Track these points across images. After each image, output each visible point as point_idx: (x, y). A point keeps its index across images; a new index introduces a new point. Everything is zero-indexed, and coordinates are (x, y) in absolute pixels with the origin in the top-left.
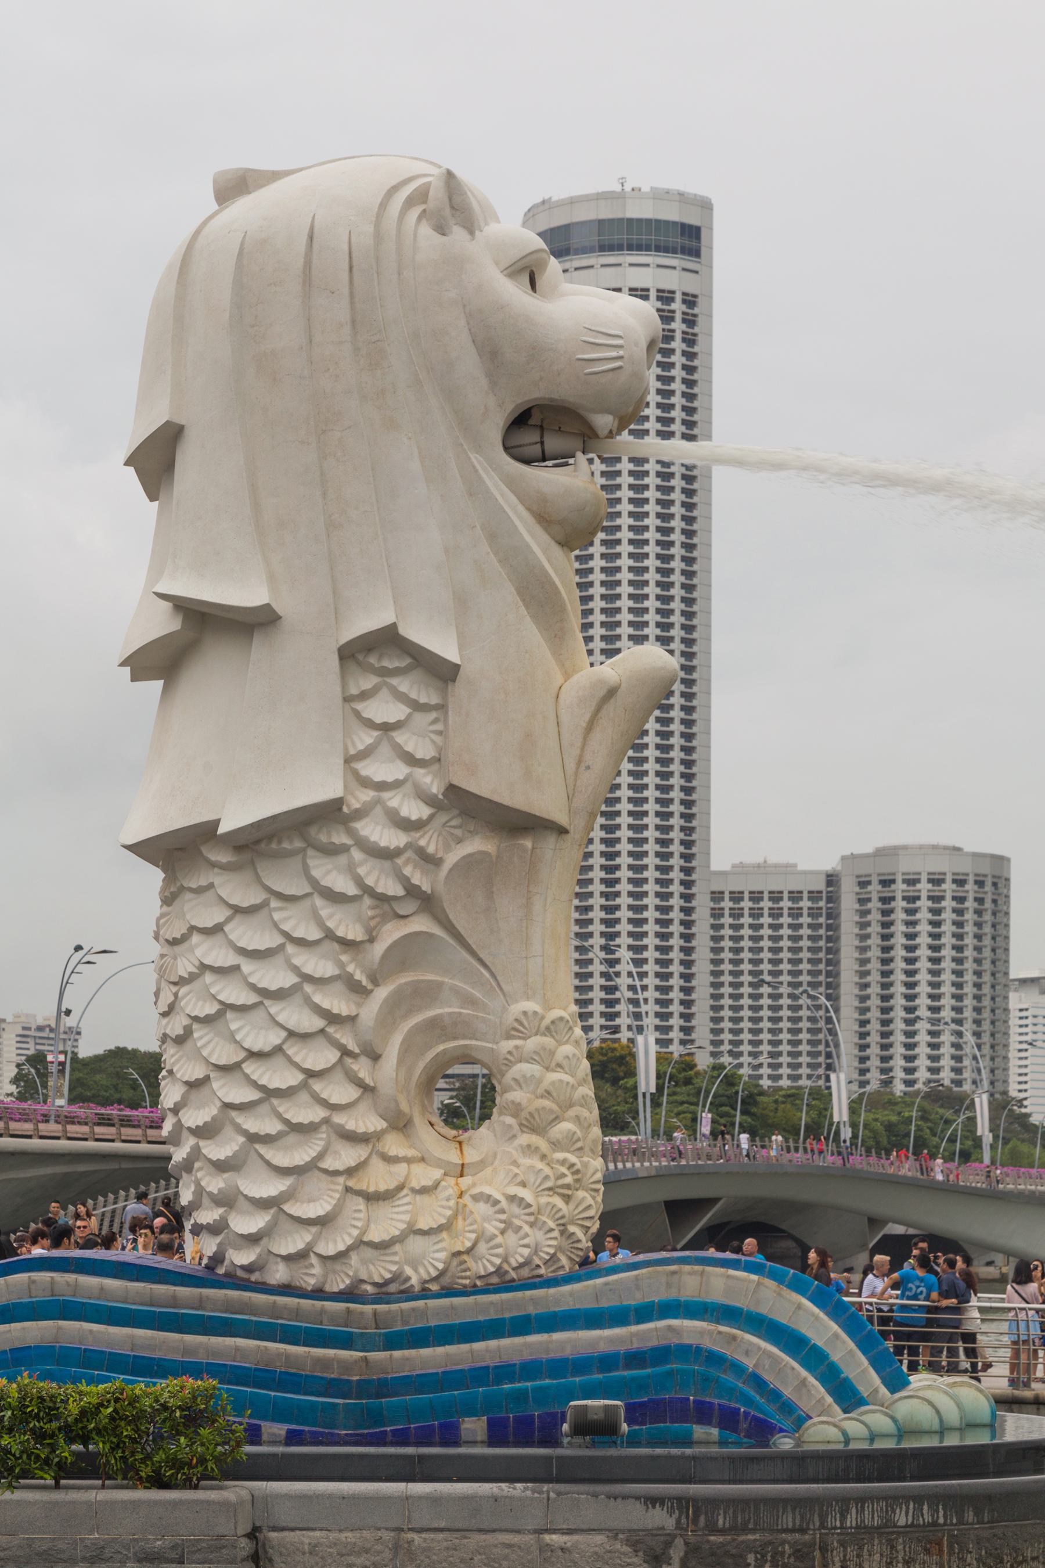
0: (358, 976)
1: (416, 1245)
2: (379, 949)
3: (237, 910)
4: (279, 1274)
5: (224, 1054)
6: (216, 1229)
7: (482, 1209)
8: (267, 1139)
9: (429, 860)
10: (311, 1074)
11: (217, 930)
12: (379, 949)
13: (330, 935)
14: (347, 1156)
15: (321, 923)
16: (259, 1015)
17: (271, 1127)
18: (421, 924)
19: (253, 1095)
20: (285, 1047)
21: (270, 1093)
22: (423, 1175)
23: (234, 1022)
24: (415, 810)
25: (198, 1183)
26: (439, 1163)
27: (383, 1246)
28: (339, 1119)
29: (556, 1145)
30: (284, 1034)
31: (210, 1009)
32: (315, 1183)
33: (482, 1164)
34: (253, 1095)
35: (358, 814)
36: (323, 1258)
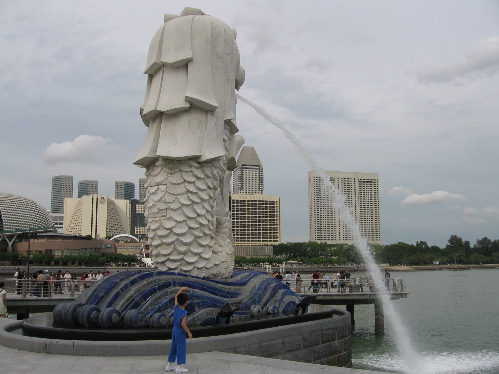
1: (222, 265)
5: (193, 215)
11: (193, 183)
16: (200, 206)
19: (197, 226)
31: (190, 203)
34: (197, 226)
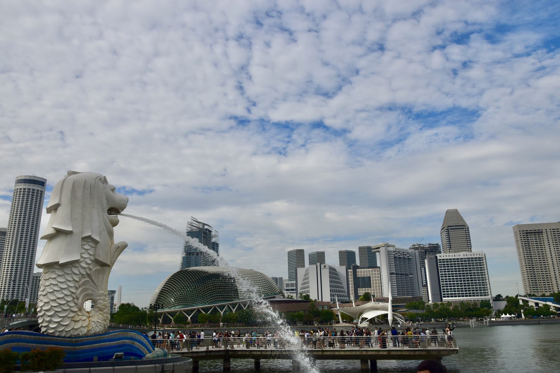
1: (82, 329)
2: (81, 282)
3: (59, 275)
4: (57, 334)
5: (53, 298)
6: (45, 327)
7: (93, 323)
8: (58, 312)
9: (90, 269)
10: (68, 301)
11: (55, 278)
12: (81, 282)
13: (74, 280)
14: (72, 315)
15: (73, 278)
17: (59, 310)
18: (87, 279)
21: (60, 304)
22: (85, 318)
24: (89, 262)
25: (44, 319)
26: (86, 316)
27: (77, 329)
28: (71, 309)
29: (104, 313)
31: (52, 290)
32: (66, 319)
33: (92, 317)
35: (81, 262)
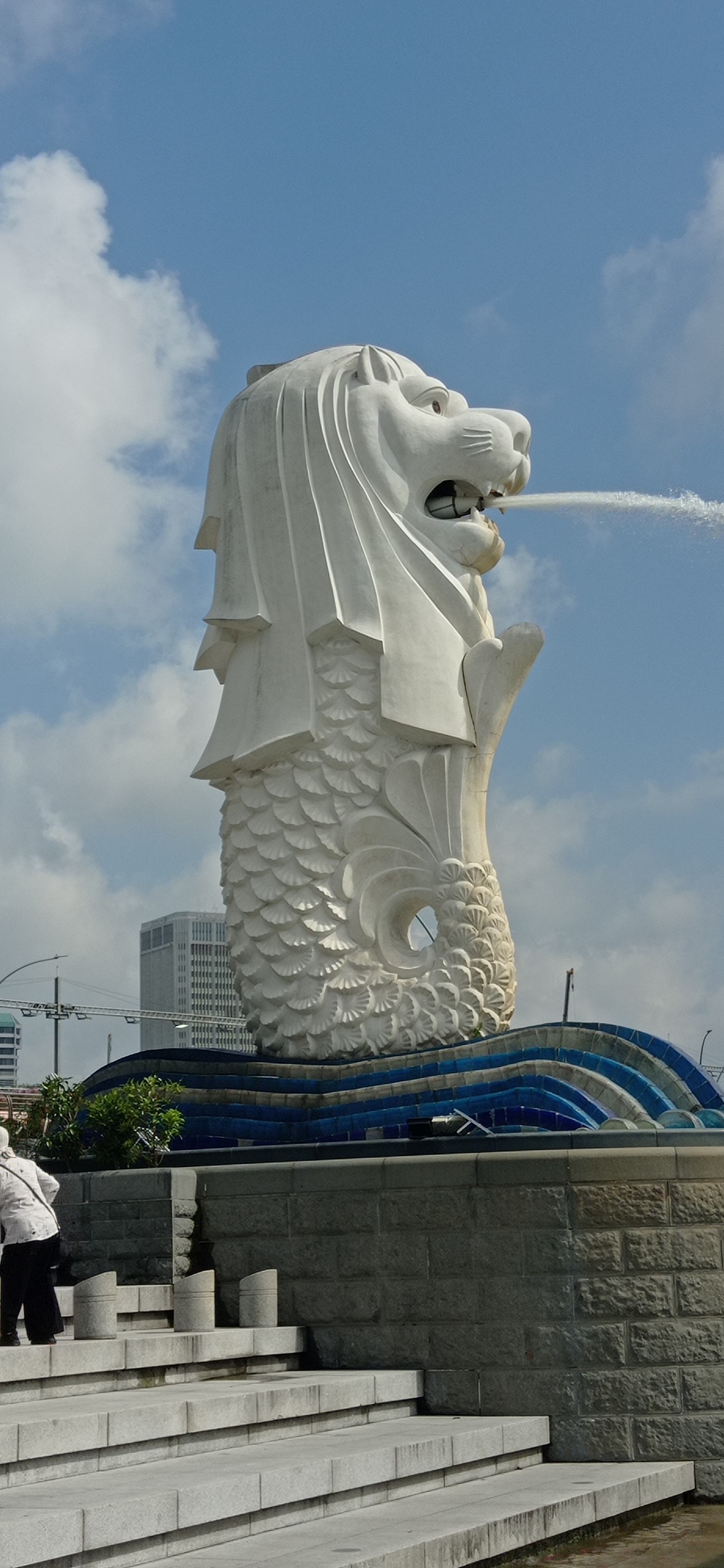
0: (331, 846)
4: (292, 1050)
18: (374, 812)
20: (285, 897)
23: (255, 884)
30: (283, 889)
35: (324, 743)
36: (315, 1037)
